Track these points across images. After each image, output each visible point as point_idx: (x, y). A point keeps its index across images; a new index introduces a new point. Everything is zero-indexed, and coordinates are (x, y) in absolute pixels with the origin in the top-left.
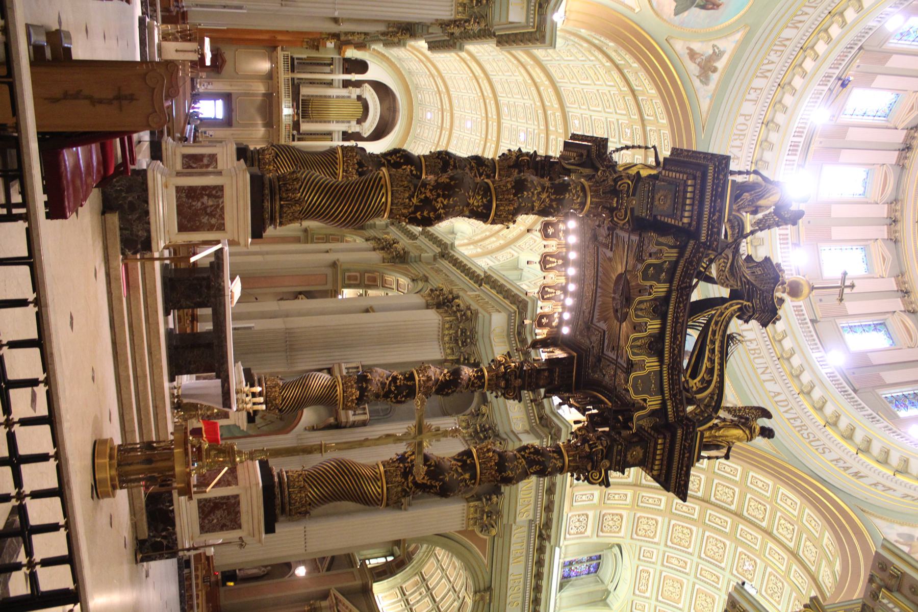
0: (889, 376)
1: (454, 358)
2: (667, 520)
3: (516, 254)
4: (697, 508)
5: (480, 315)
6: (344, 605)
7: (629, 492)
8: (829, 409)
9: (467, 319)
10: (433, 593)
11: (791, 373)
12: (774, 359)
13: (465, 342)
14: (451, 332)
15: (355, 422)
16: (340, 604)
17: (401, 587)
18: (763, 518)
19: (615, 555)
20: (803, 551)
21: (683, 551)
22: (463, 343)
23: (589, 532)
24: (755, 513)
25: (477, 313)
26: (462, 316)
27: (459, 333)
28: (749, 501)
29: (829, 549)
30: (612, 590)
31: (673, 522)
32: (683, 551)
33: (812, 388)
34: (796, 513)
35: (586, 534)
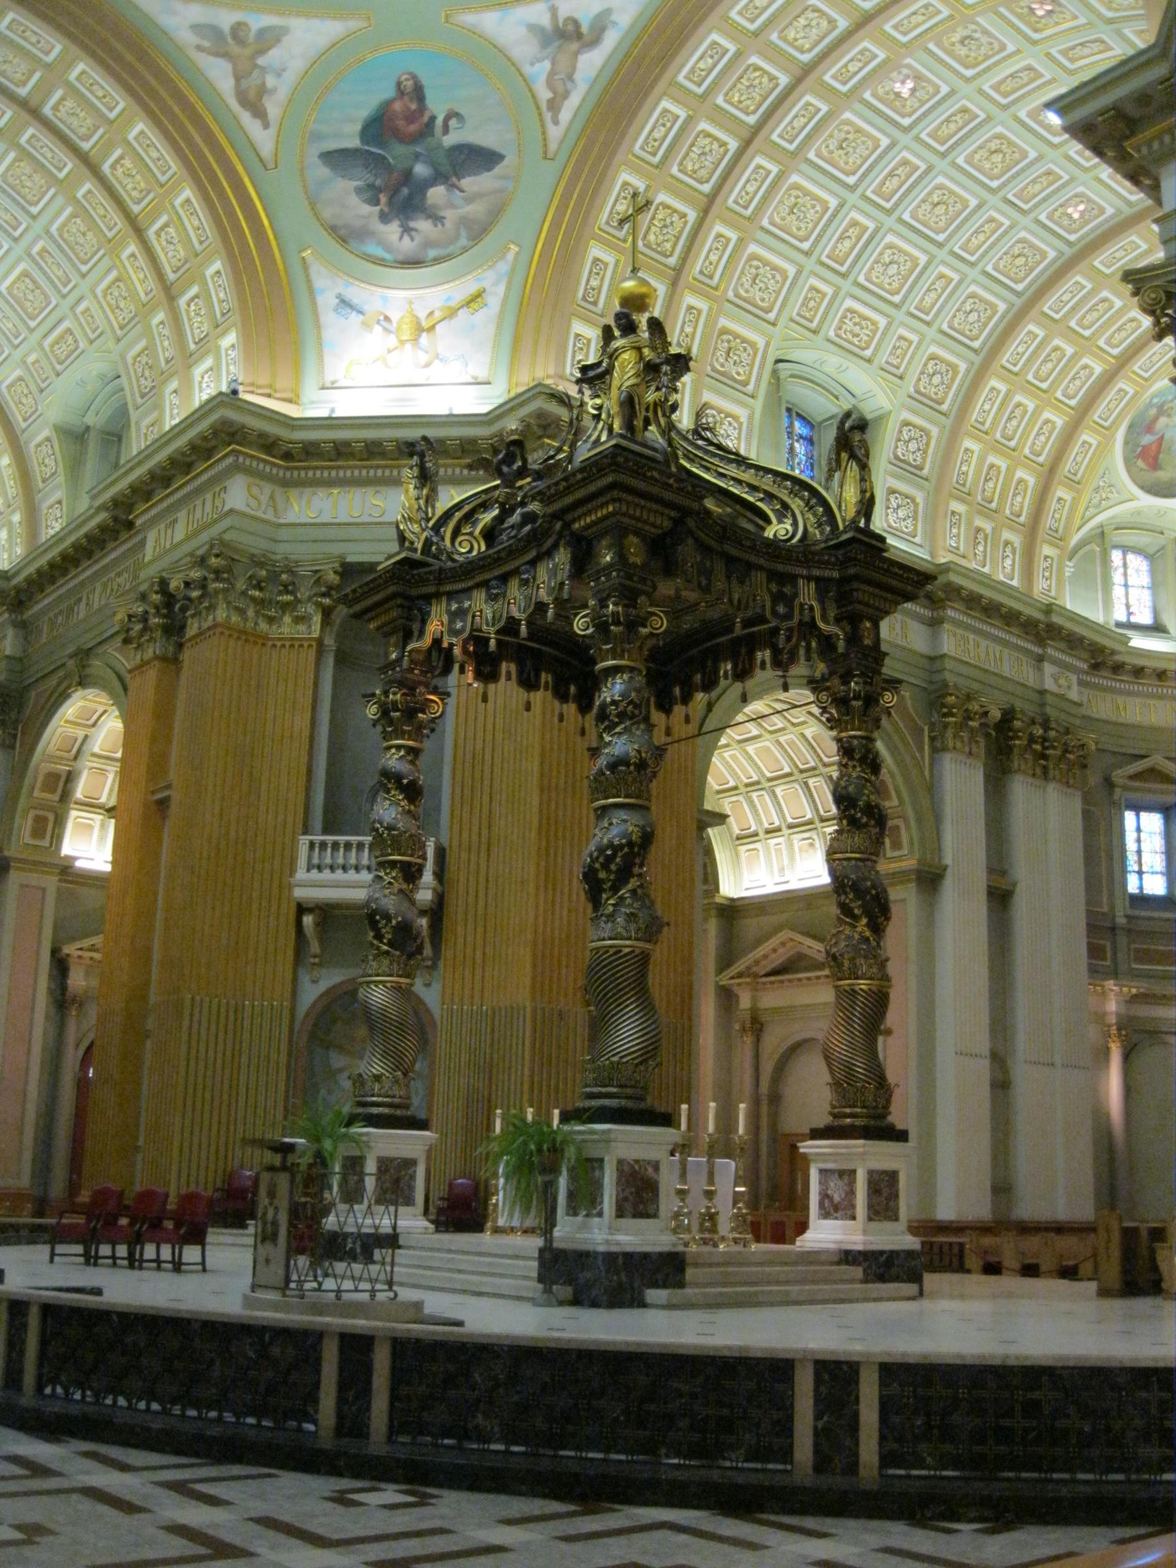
1: (317, 619)
3: (46, 433)
4: (759, 160)
5: (227, 537)
6: (757, 962)
7: (690, 299)
9: (229, 570)
10: (769, 775)
13: (286, 586)
14: (251, 613)
15: (434, 873)
16: (755, 969)
17: (738, 838)
19: (792, 376)
21: (830, 221)
22: (288, 592)
23: (742, 413)
24: (814, 33)
25: (223, 543)
26: (217, 579)
27: (257, 593)
28: (785, 40)
30: (853, 401)
31: (765, 223)
32: (830, 221)
35: (743, 419)
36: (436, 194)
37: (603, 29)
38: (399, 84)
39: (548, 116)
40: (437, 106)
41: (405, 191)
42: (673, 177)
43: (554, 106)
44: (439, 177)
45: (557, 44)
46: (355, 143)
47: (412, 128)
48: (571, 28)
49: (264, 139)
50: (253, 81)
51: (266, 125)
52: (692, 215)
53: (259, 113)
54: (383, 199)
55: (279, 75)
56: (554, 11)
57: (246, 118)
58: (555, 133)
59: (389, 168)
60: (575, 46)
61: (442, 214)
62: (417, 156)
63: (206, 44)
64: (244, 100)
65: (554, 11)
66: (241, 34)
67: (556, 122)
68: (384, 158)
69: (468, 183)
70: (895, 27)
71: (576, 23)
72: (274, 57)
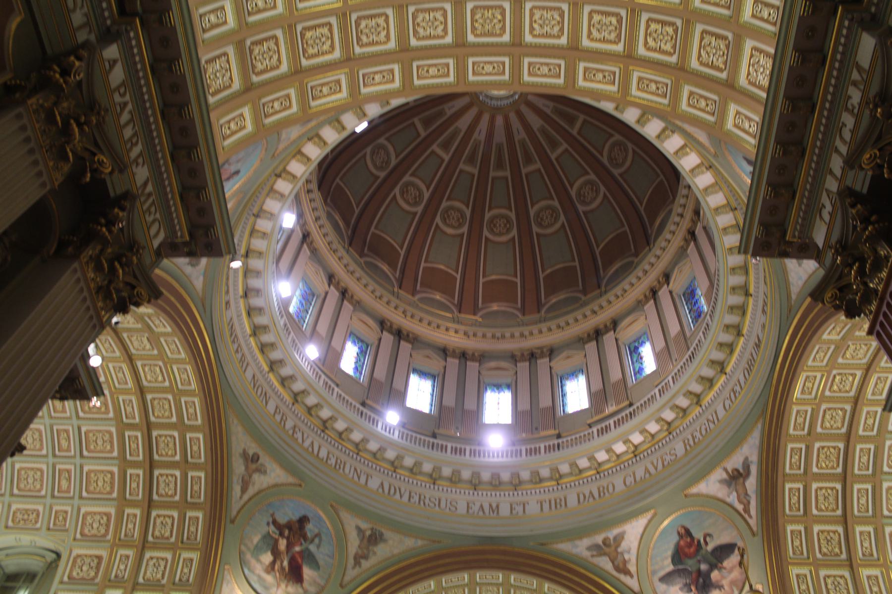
0: (674, 328)
2: (885, 521)
4: (856, 487)
8: (708, 372)
11: (682, 417)
12: (671, 437)
18: (841, 409)
20: (860, 359)
29: (840, 332)
33: (691, 393)
34: (819, 375)
36: (715, 575)
37: (748, 467)
38: (679, 533)
39: (746, 516)
40: (698, 535)
41: (701, 580)
42: (816, 516)
43: (747, 510)
44: (713, 567)
45: (734, 483)
46: (671, 568)
47: (692, 550)
48: (736, 473)
49: (633, 583)
50: (620, 558)
51: (632, 576)
52: (840, 529)
53: (627, 573)
54: (693, 588)
55: (629, 552)
56: (726, 470)
57: (622, 577)
58: (753, 522)
59: (690, 573)
60: (741, 480)
61: (720, 584)
62: (699, 562)
63: (595, 553)
64: (617, 569)
65: (726, 470)
66: (608, 542)
67: (750, 517)
68: (686, 570)
69: (726, 564)
70: (873, 394)
71: (737, 470)
72: (624, 545)
